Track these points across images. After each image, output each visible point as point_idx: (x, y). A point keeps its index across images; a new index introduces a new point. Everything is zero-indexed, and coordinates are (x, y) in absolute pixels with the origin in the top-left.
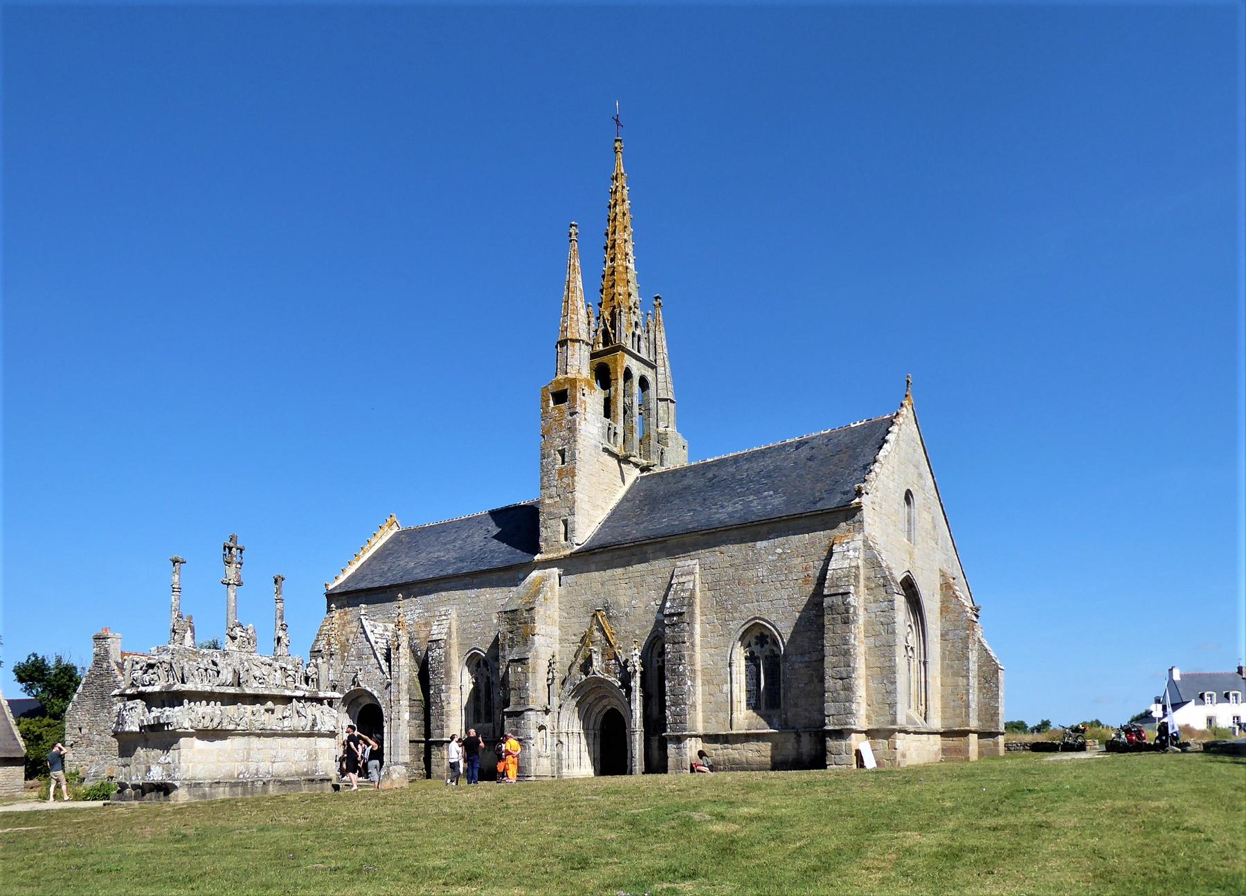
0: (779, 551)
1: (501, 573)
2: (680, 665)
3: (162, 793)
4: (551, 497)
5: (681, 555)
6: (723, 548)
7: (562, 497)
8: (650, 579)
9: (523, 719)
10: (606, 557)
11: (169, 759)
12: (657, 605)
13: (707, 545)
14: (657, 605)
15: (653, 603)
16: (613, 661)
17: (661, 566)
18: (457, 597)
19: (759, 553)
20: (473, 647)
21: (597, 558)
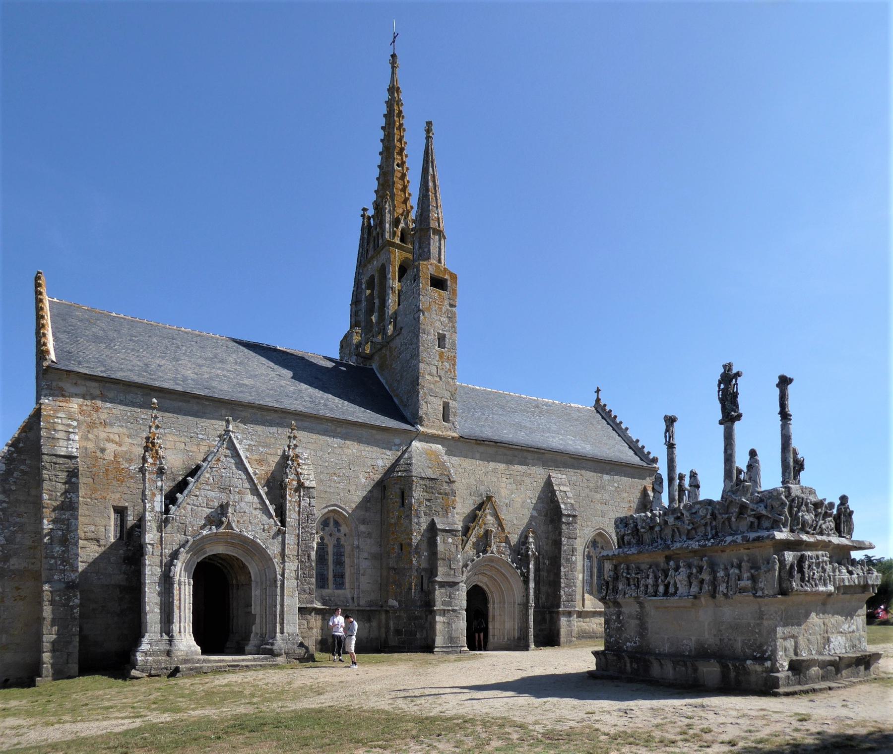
0: (616, 485)
1: (374, 432)
2: (572, 555)
3: (862, 668)
4: (431, 374)
5: (553, 468)
6: (583, 472)
7: (443, 379)
8: (527, 480)
9: (458, 590)
10: (491, 450)
11: (854, 627)
12: (532, 503)
13: (573, 467)
14: (532, 503)
15: (529, 501)
16: (504, 544)
17: (537, 472)
18: (313, 441)
19: (605, 483)
20: (332, 503)
21: (482, 449)
